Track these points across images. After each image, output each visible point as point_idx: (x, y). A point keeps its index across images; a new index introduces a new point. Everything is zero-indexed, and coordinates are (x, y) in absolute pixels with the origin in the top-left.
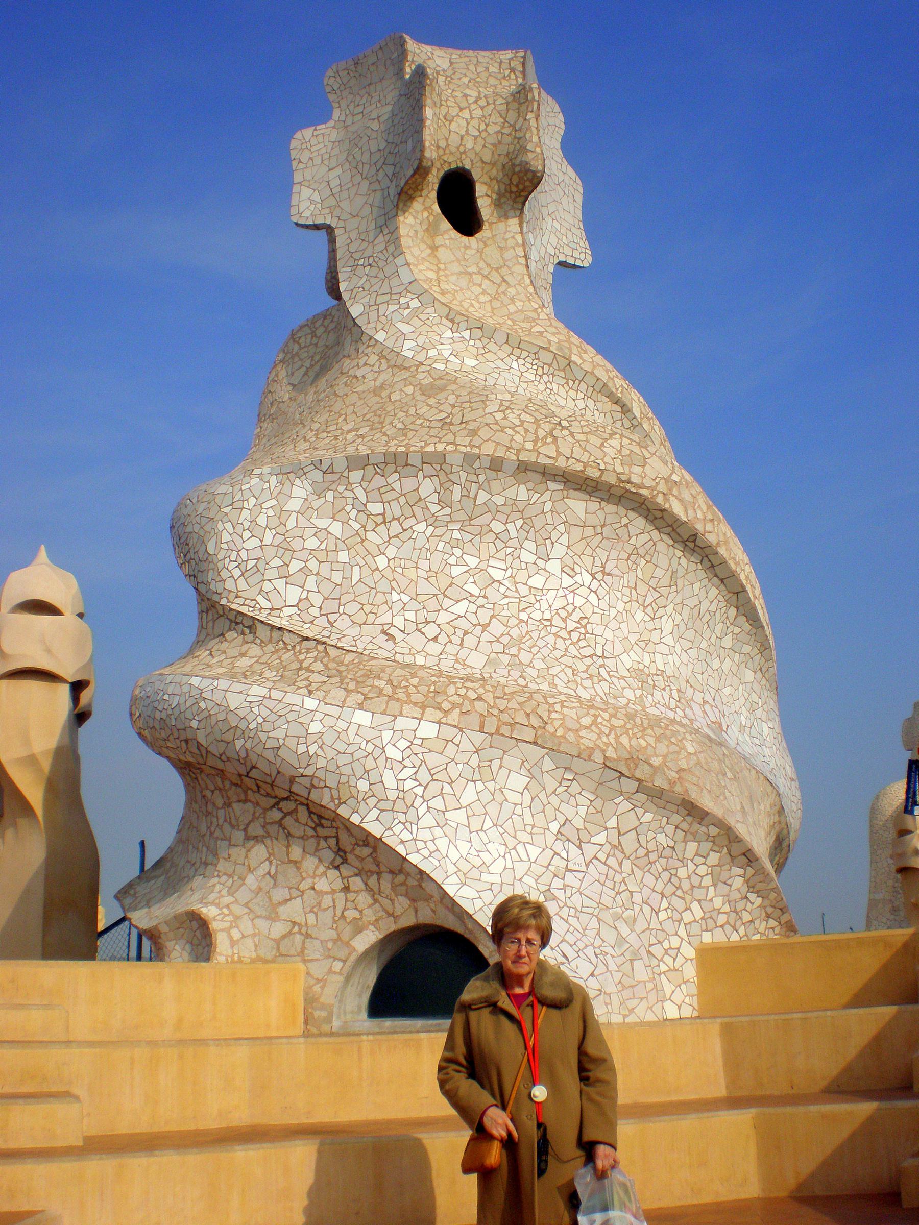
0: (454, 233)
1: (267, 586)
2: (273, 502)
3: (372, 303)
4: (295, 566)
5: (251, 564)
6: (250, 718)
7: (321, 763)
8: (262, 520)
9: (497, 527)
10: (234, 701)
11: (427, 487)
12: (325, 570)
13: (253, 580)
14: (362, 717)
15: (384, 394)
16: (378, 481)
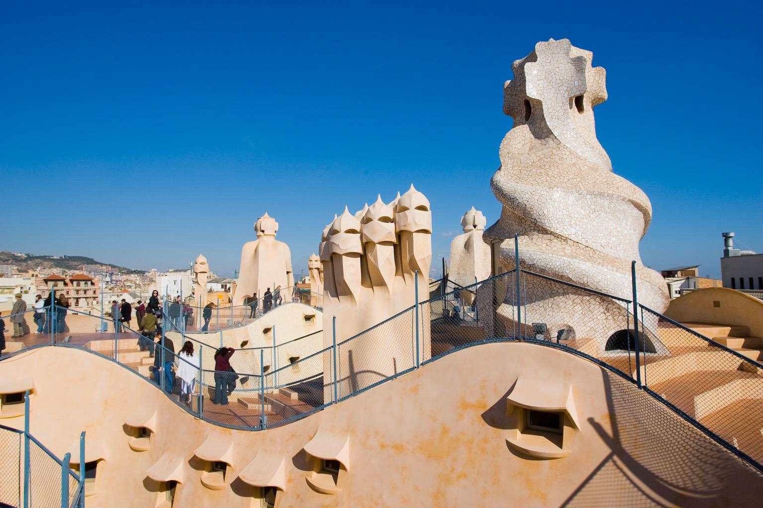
0: (578, 112)
1: (565, 227)
2: (564, 201)
3: (561, 132)
4: (573, 222)
5: (560, 220)
6: (590, 272)
7: (611, 287)
8: (561, 206)
9: (619, 216)
10: (583, 267)
11: (606, 203)
12: (581, 223)
13: (562, 224)
14: (618, 274)
15: (578, 167)
16: (595, 199)
